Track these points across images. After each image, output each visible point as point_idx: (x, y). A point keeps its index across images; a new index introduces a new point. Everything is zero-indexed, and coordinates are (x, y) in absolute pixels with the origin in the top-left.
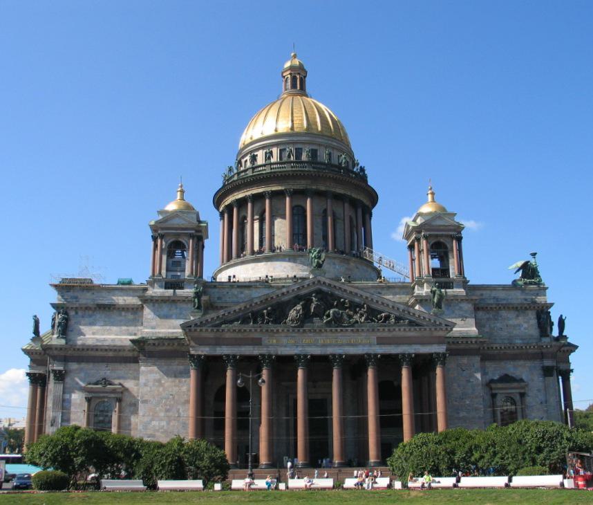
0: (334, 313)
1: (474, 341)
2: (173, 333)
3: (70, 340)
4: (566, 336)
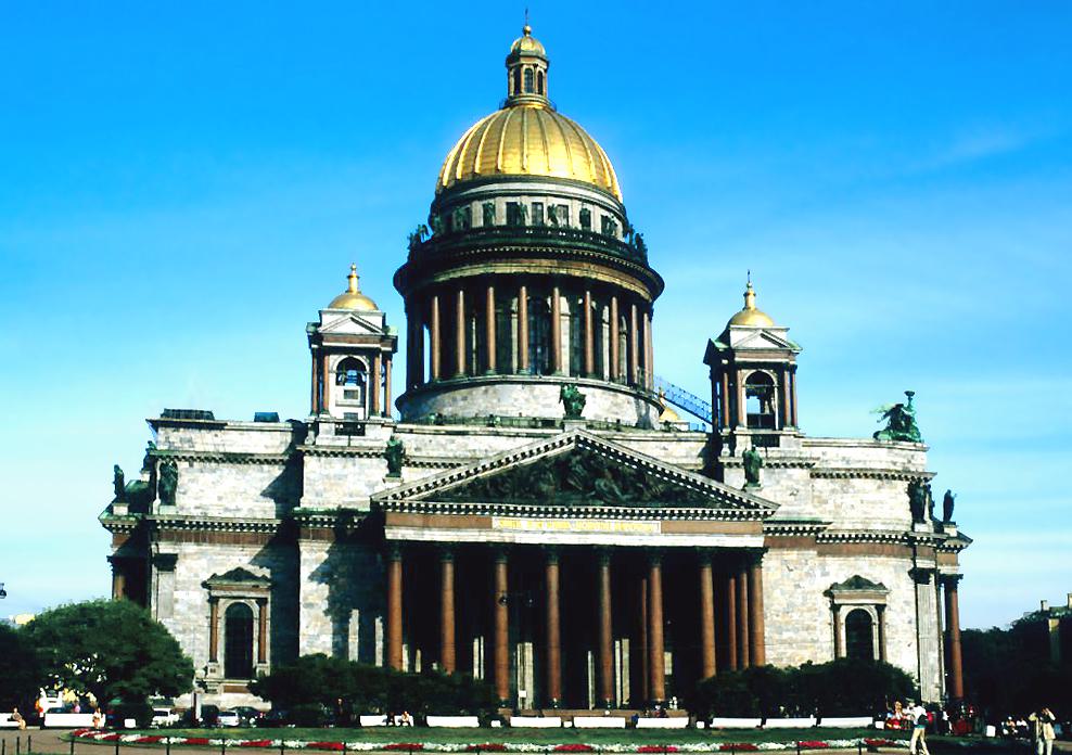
1: (808, 527)
2: (350, 503)
3: (182, 508)
4: (954, 523)
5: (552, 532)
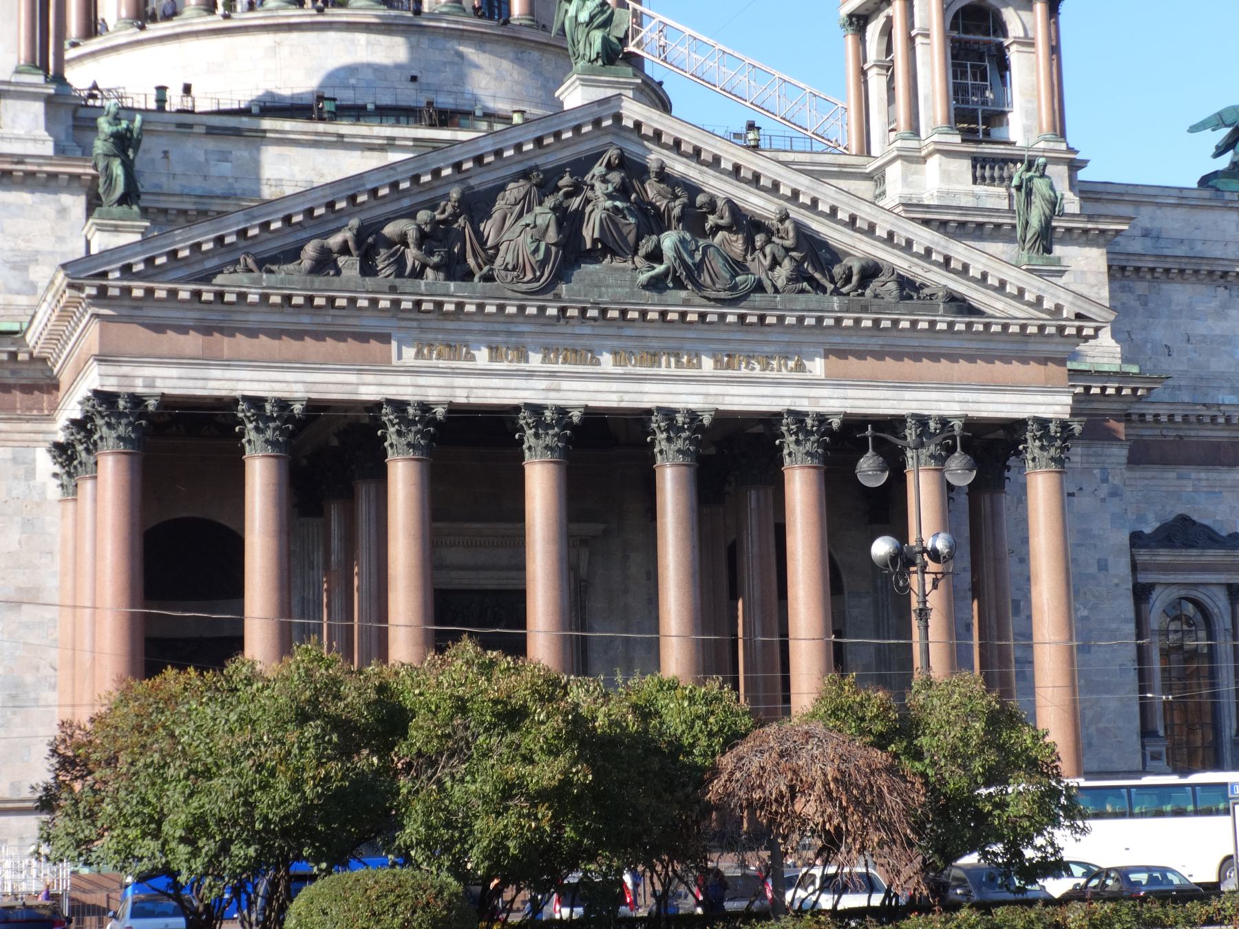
0: (677, 250)
5: (552, 375)
